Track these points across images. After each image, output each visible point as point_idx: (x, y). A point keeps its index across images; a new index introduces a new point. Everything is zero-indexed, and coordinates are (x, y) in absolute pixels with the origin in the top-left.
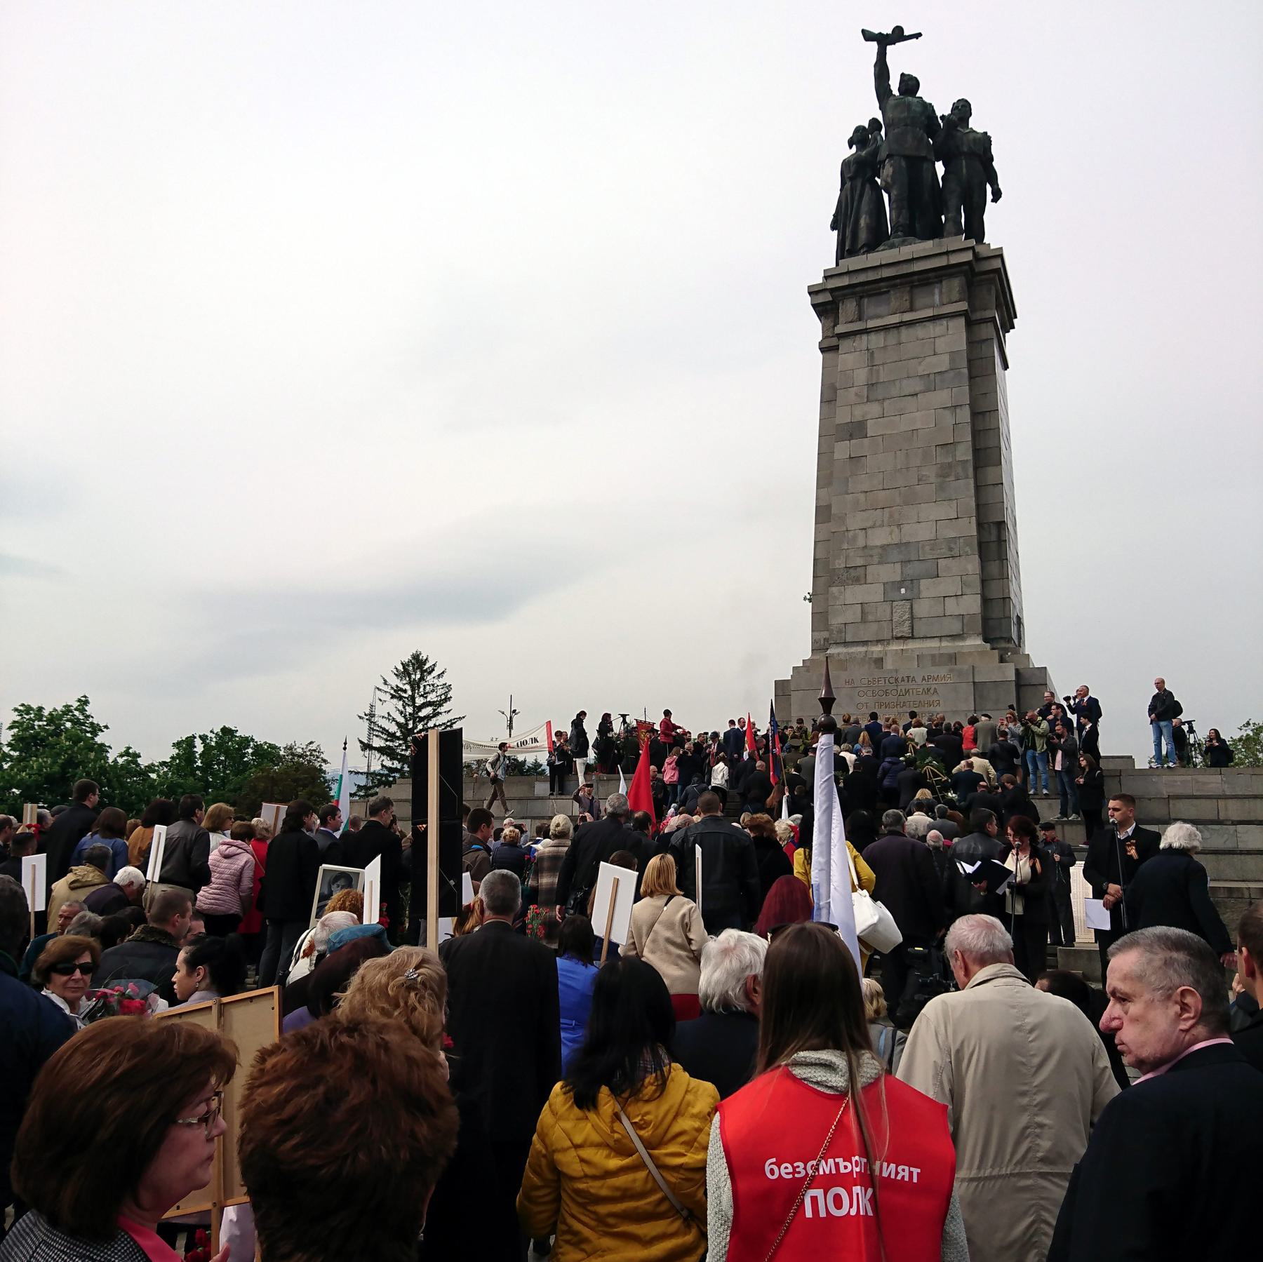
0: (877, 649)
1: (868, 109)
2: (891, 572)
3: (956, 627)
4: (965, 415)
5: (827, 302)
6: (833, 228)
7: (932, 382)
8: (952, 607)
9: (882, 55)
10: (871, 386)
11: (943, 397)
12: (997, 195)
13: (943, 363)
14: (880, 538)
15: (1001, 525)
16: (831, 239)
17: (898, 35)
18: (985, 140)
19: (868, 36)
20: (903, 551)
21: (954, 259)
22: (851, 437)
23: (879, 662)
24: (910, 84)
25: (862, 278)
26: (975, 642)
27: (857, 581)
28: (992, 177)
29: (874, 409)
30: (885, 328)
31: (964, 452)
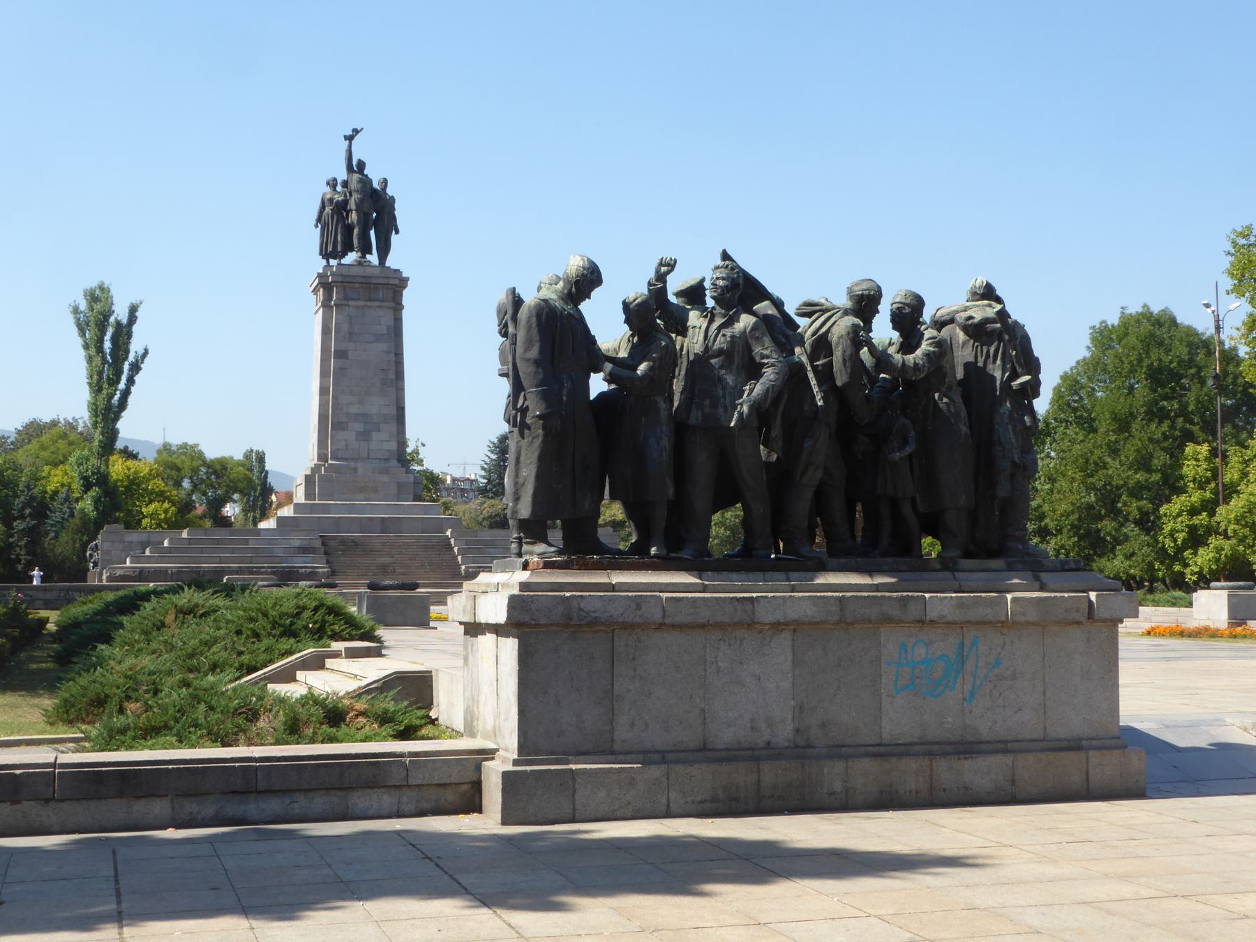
0: (352, 464)
1: (342, 175)
2: (359, 427)
3: (387, 455)
4: (392, 357)
5: (325, 284)
6: (316, 226)
7: (378, 338)
8: (386, 446)
9: (350, 146)
10: (351, 334)
11: (383, 346)
12: (397, 232)
13: (383, 329)
14: (354, 410)
15: (403, 409)
16: (317, 232)
17: (356, 131)
18: (393, 199)
19: (346, 138)
20: (364, 417)
21: (392, 281)
22: (340, 358)
23: (355, 469)
24: (361, 165)
25: (348, 279)
26: (394, 462)
27: (343, 429)
28: (394, 218)
29: (351, 346)
30: (357, 307)
31: (392, 375)
